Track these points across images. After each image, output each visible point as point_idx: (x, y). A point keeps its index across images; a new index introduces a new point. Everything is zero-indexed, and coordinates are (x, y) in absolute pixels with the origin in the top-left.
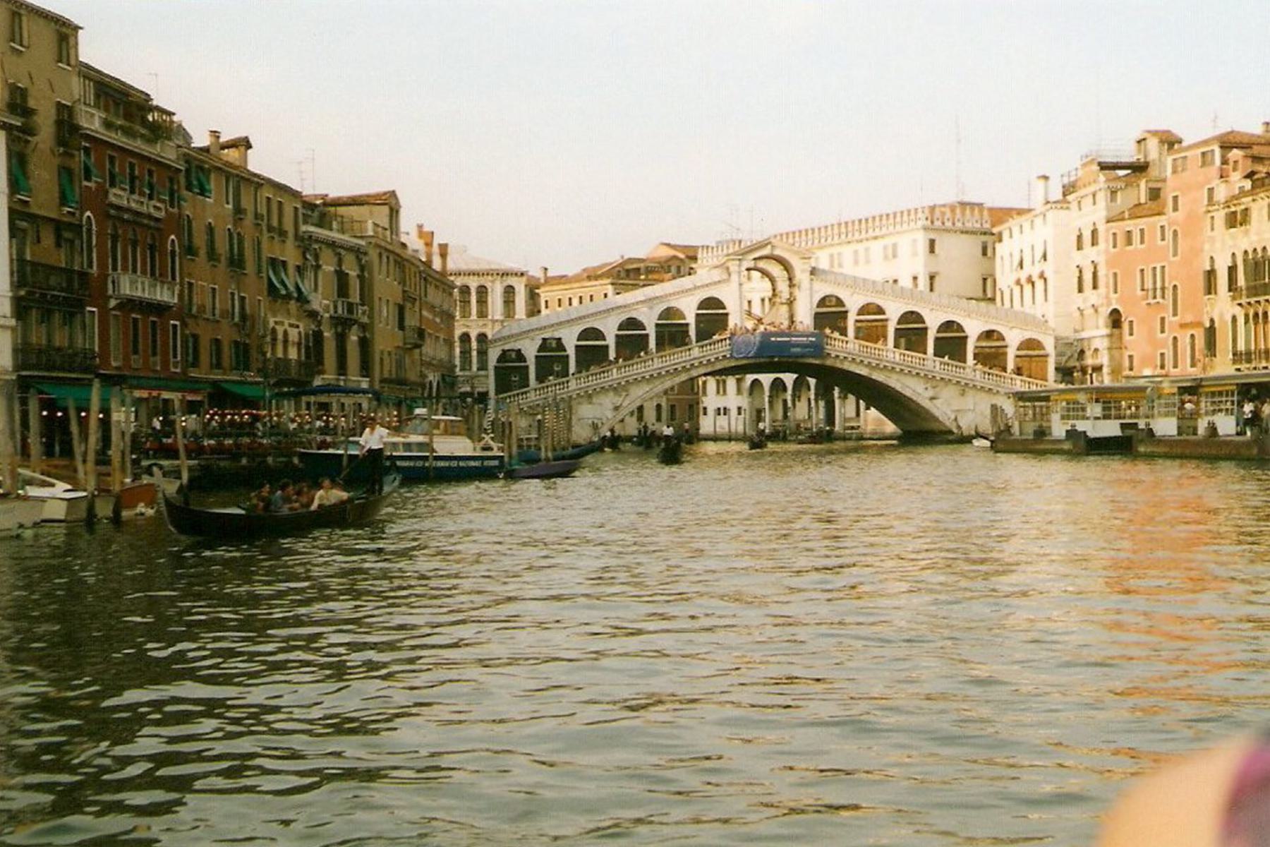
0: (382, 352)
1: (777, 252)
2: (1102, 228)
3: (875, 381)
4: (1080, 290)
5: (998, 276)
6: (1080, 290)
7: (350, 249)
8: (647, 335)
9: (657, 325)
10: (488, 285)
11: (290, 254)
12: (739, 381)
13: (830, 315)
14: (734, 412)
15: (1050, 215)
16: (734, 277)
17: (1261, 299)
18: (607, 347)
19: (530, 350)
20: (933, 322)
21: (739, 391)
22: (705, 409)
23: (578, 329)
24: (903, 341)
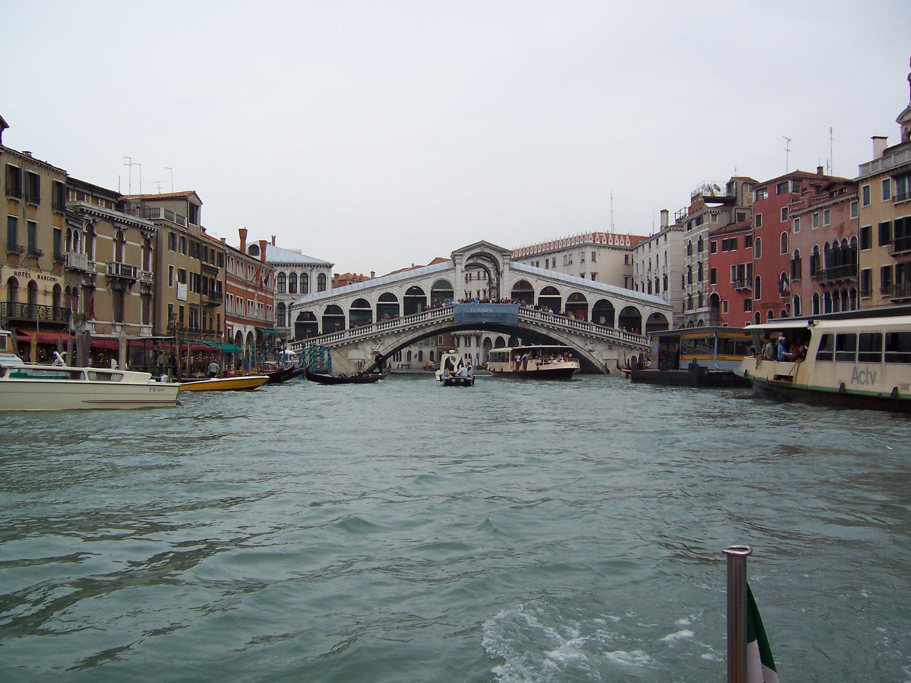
1: (487, 250)
2: (705, 239)
5: (635, 274)
6: (690, 282)
7: (134, 226)
8: (398, 305)
10: (308, 273)
12: (478, 338)
13: (523, 292)
14: (474, 357)
15: (668, 235)
17: (842, 279)
19: (319, 313)
20: (592, 300)
21: (478, 345)
23: (351, 300)
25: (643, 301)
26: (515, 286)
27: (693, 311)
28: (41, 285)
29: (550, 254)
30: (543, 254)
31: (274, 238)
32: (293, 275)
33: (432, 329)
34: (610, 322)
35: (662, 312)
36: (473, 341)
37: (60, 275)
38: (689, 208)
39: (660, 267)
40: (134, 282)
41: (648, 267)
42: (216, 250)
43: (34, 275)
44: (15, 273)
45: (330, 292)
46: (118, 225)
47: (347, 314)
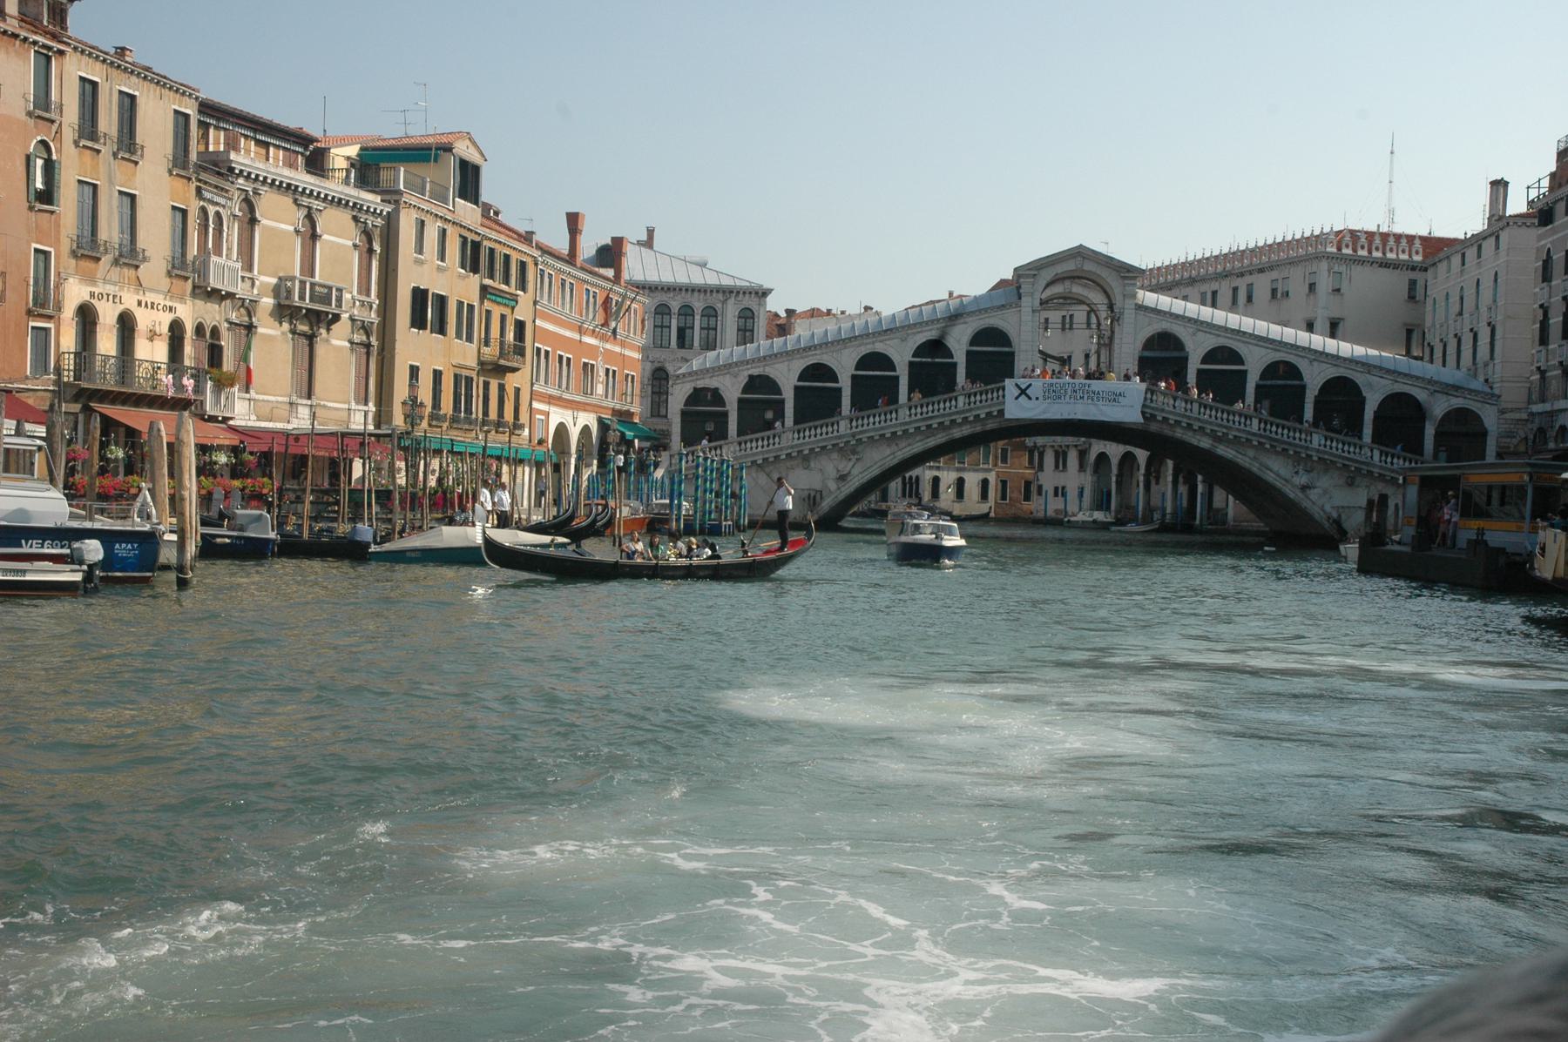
0: (414, 371)
1: (1089, 266)
3: (1220, 457)
4: (1544, 340)
5: (1428, 323)
7: (339, 203)
8: (897, 378)
9: (911, 364)
11: (155, 185)
12: (1083, 454)
14: (1072, 494)
15: (1504, 236)
16: (1026, 301)
18: (839, 390)
20: (1314, 377)
21: (1082, 467)
22: (1040, 488)
23: (799, 365)
24: (1266, 403)
25: (1430, 381)
26: (1149, 344)
27: (1547, 407)
28: (143, 319)
29: (1242, 275)
30: (1226, 275)
31: (651, 232)
32: (687, 311)
33: (966, 431)
34: (1355, 427)
35: (1473, 406)
36: (1073, 458)
37: (182, 299)
38: (1553, 176)
39: (1483, 309)
40: (337, 318)
41: (1458, 306)
42: (514, 256)
43: (129, 301)
44: (92, 295)
45: (762, 344)
46: (305, 201)
47: (788, 395)
